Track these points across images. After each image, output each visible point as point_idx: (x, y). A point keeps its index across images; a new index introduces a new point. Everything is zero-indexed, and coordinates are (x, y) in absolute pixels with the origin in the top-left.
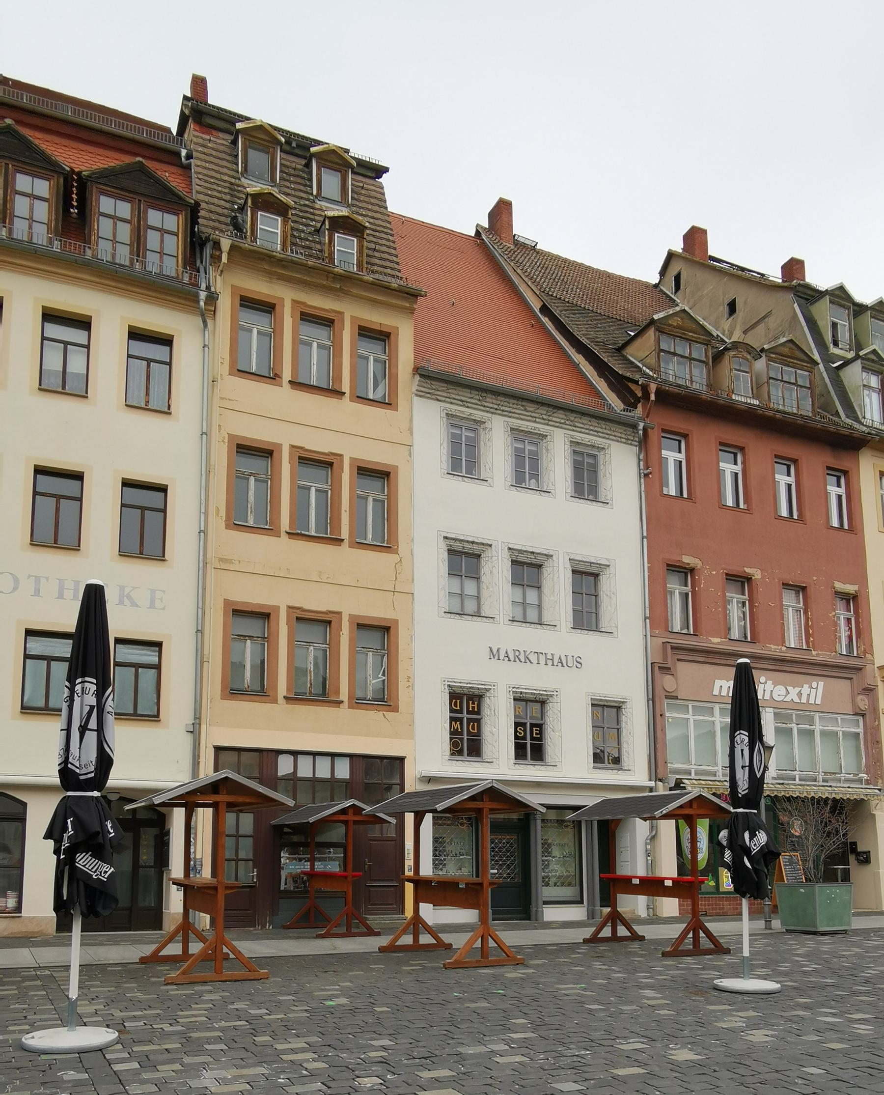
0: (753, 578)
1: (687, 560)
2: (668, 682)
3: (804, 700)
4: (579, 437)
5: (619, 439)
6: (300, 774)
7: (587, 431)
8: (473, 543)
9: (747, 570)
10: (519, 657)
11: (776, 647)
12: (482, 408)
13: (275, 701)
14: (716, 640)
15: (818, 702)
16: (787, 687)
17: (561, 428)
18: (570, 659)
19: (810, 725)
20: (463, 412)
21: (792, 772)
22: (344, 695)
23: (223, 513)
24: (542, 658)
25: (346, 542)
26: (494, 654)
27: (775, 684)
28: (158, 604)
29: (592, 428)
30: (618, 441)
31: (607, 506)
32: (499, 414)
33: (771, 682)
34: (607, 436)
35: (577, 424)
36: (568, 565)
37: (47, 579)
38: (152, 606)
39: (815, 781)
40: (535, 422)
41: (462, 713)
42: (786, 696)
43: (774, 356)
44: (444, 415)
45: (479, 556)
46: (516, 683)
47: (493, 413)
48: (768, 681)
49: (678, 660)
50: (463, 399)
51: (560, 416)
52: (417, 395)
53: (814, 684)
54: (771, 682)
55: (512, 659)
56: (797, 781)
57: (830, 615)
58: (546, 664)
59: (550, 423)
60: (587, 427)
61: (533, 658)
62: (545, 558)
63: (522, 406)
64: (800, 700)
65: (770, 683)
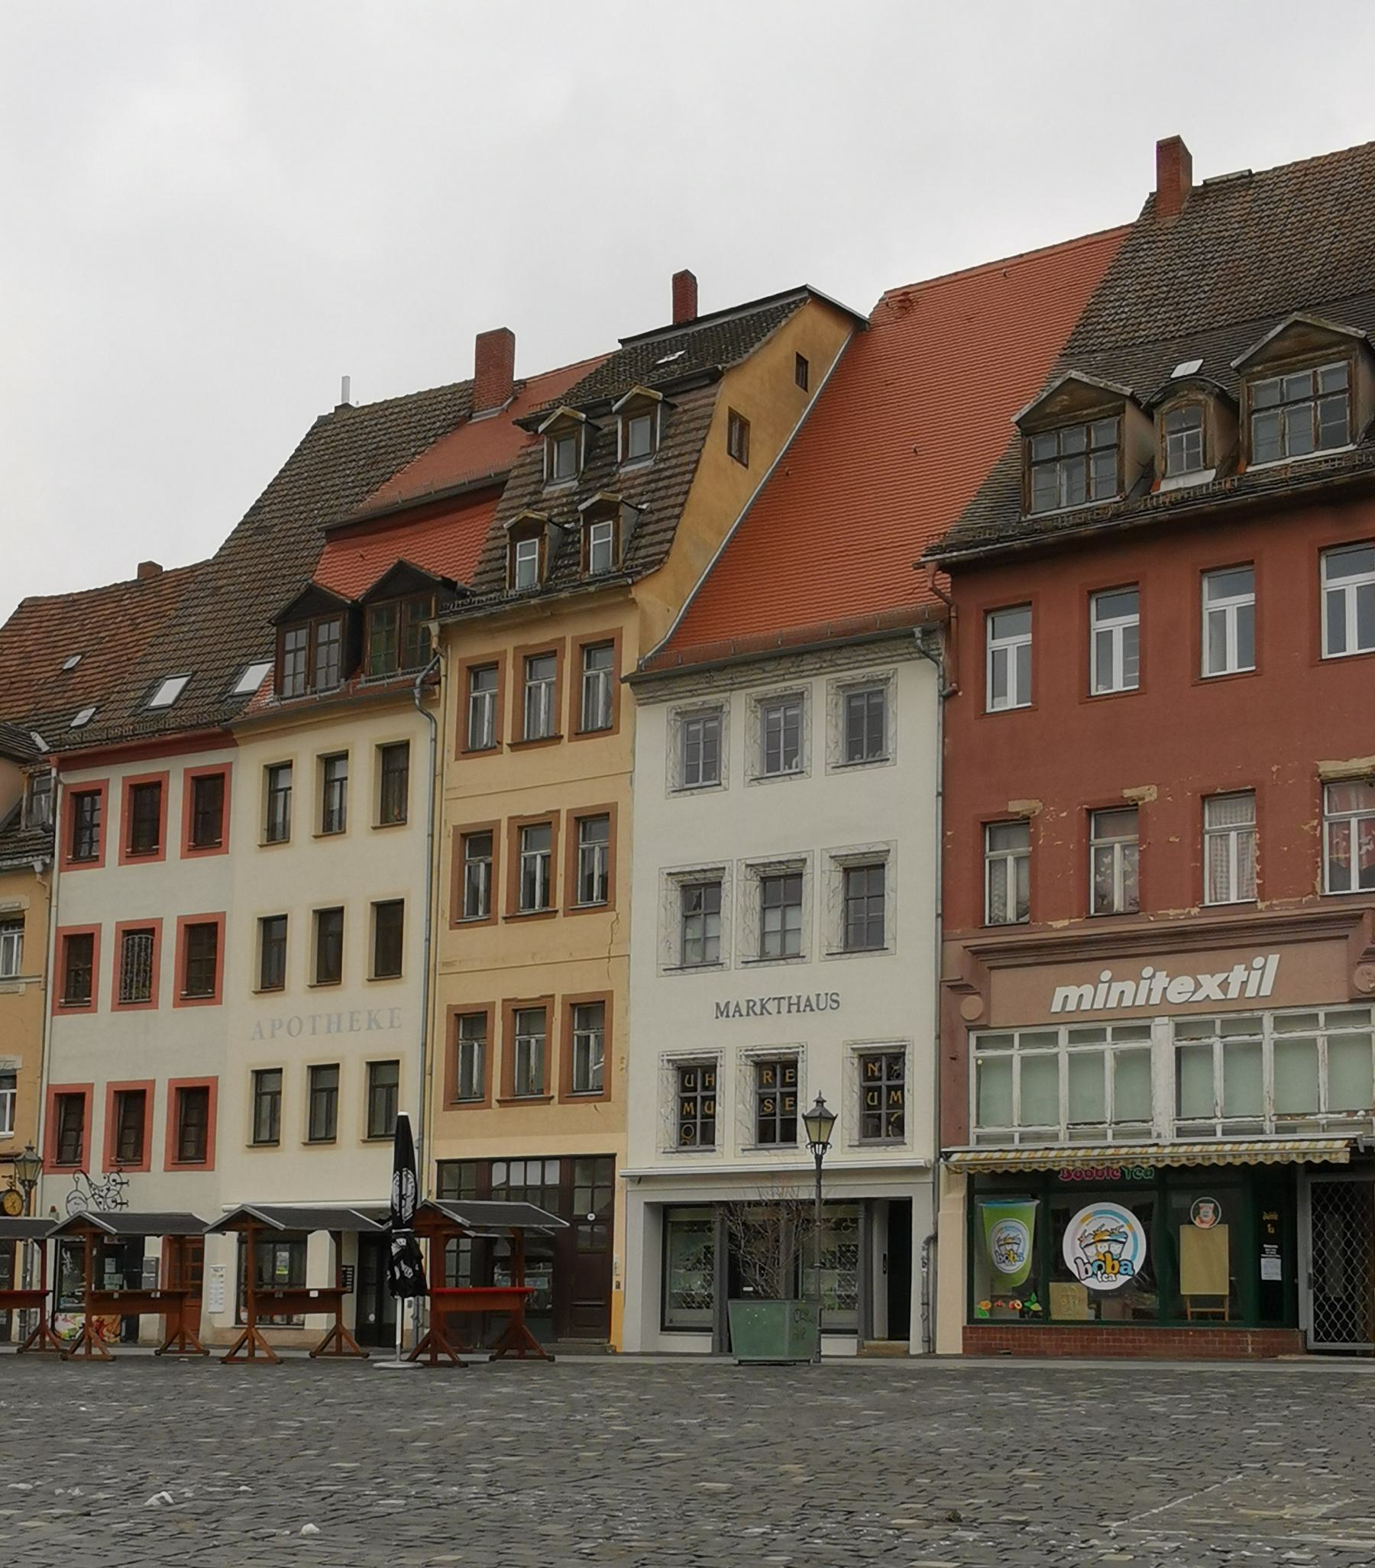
0: (1140, 803)
1: (1016, 806)
2: (970, 1007)
3: (1233, 993)
4: (847, 676)
5: (908, 656)
6: (548, 1182)
7: (857, 665)
8: (705, 871)
9: (1128, 793)
10: (757, 1009)
11: (1179, 911)
12: (715, 689)
13: (490, 1107)
14: (1058, 924)
15: (1266, 991)
16: (1199, 977)
17: (821, 674)
18: (822, 998)
19: (1251, 1035)
20: (693, 704)
21: (1208, 1121)
22: (554, 1091)
23: (447, 915)
24: (784, 1004)
25: (561, 913)
26: (722, 1011)
27: (1172, 977)
28: (396, 1024)
29: (861, 658)
30: (909, 660)
31: (888, 763)
32: (739, 689)
33: (1165, 973)
34: (889, 660)
35: (839, 662)
36: (830, 865)
37: (320, 1016)
38: (392, 1026)
39: (1262, 1132)
40: (784, 680)
41: (696, 1090)
42: (1194, 993)
43: (1259, 368)
44: (672, 716)
45: (720, 883)
46: (750, 1044)
47: (731, 690)
48: (1158, 974)
49: (991, 968)
50: (688, 688)
51: (809, 663)
52: (640, 705)
53: (1258, 962)
54: (1165, 973)
55: (744, 1012)
56: (1219, 1137)
57: (1306, 828)
58: (789, 1011)
59: (803, 674)
60: (855, 659)
61: (772, 1006)
62: (800, 864)
63: (759, 668)
64: (1226, 995)
65: (1162, 975)
